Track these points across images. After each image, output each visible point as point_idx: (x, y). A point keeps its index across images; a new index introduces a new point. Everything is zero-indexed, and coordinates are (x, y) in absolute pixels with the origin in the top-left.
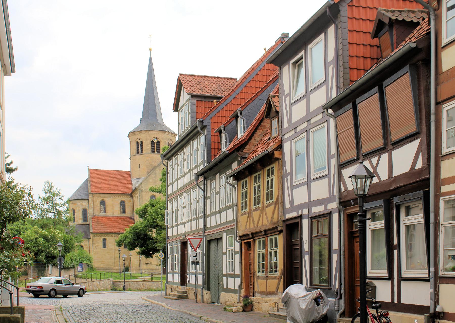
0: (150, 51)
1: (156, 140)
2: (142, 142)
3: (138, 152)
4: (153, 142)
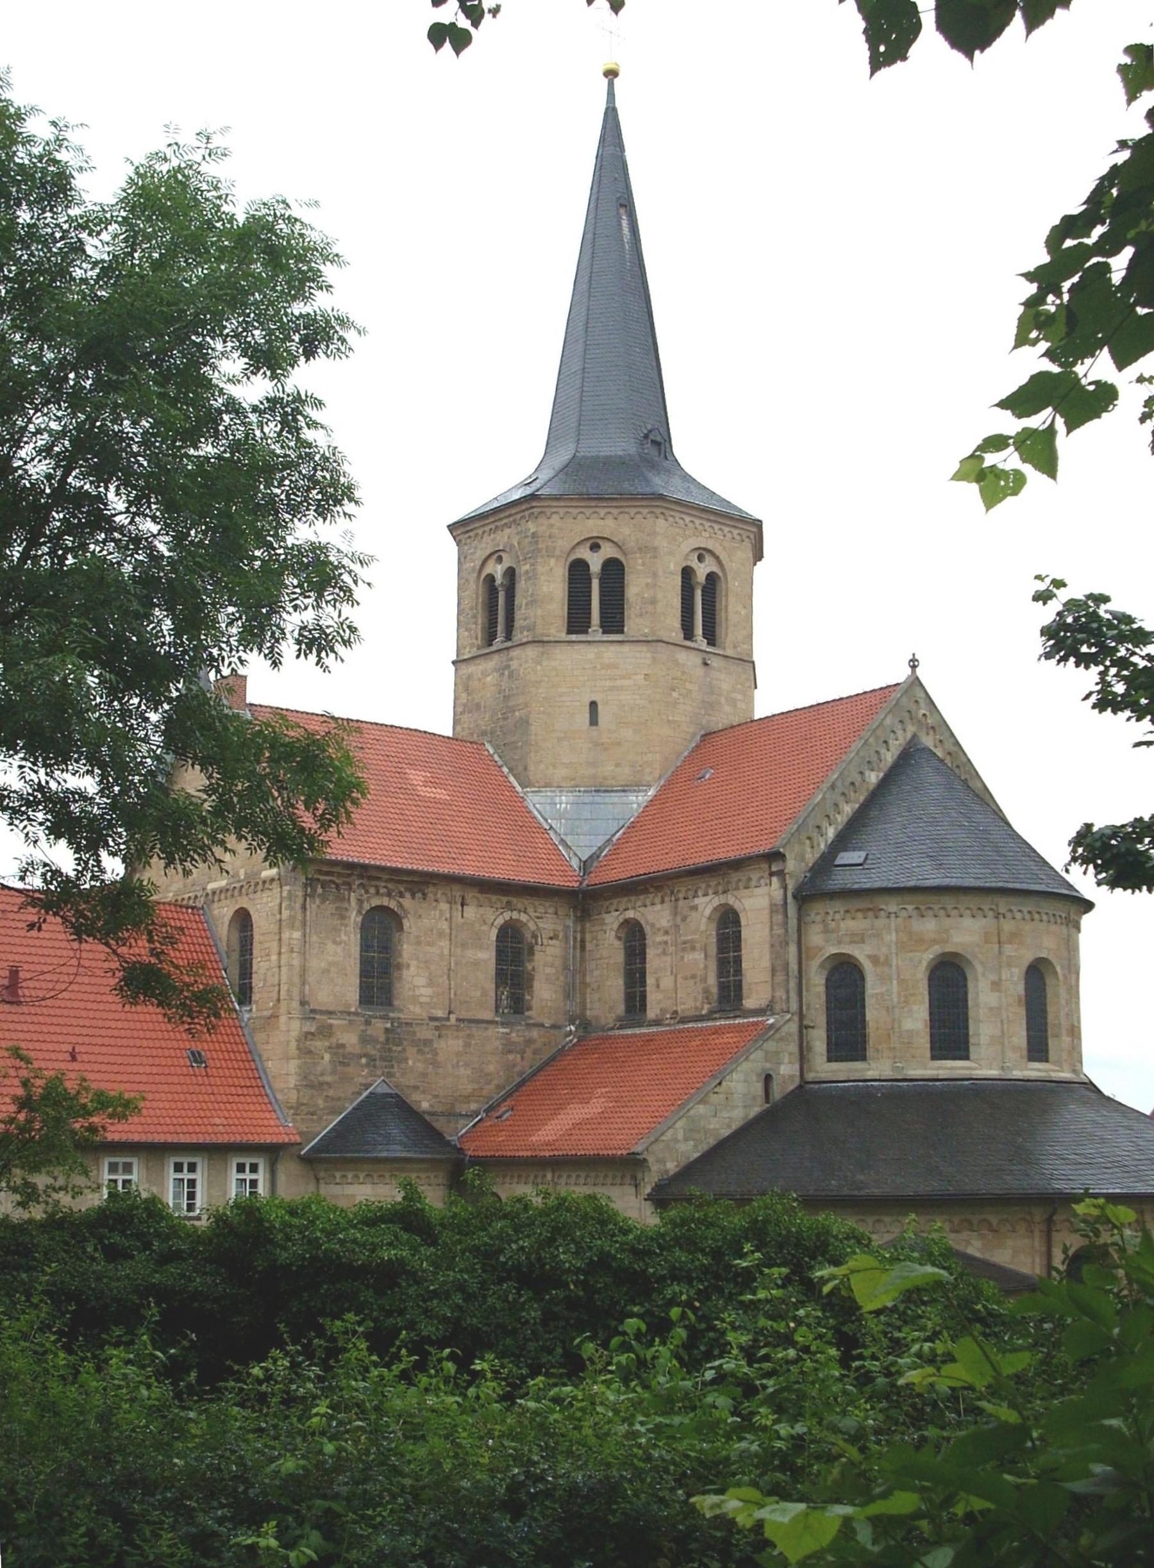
0: (605, 81)
1: (702, 571)
2: (511, 573)
3: (490, 637)
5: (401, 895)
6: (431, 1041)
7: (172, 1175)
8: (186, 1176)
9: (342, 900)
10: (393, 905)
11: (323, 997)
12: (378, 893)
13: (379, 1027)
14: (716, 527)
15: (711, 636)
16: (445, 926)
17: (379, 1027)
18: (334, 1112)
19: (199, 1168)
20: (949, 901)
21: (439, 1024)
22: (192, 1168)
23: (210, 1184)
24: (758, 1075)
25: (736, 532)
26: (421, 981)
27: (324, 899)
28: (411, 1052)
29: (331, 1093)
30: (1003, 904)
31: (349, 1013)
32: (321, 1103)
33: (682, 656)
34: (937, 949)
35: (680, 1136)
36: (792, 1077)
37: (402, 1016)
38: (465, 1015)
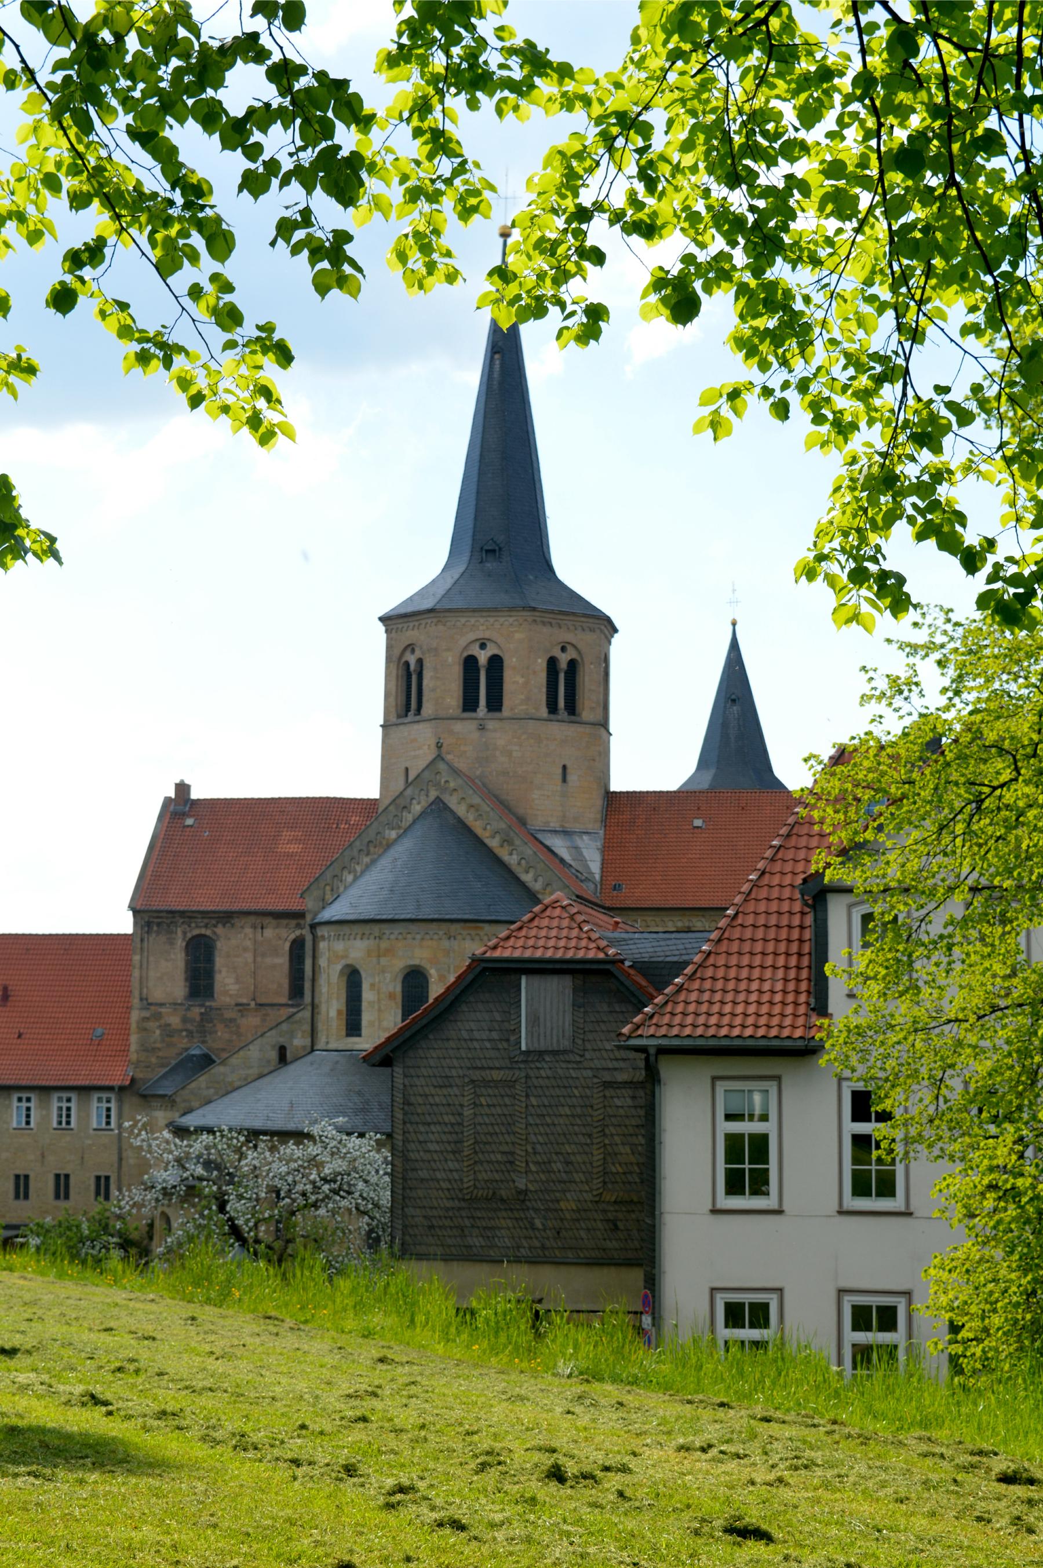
4: (470, 663)
5: (215, 926)
6: (235, 1020)
7: (15, 1104)
8: (64, 1105)
9: (172, 932)
10: (208, 932)
11: (158, 994)
12: (197, 927)
13: (196, 1012)
14: (491, 620)
15: (495, 703)
16: (249, 943)
17: (196, 1012)
18: (163, 1066)
19: (113, 1101)
20: (346, 929)
21: (242, 1008)
22: (28, 1100)
23: (79, 1110)
24: (273, 1046)
25: (511, 620)
26: (230, 980)
27: (158, 933)
28: (220, 1027)
29: (160, 1054)
30: (376, 929)
31: (175, 1004)
32: (154, 1060)
33: (458, 727)
34: (343, 962)
35: (203, 1085)
36: (304, 1047)
37: (213, 1004)
38: (263, 1001)
